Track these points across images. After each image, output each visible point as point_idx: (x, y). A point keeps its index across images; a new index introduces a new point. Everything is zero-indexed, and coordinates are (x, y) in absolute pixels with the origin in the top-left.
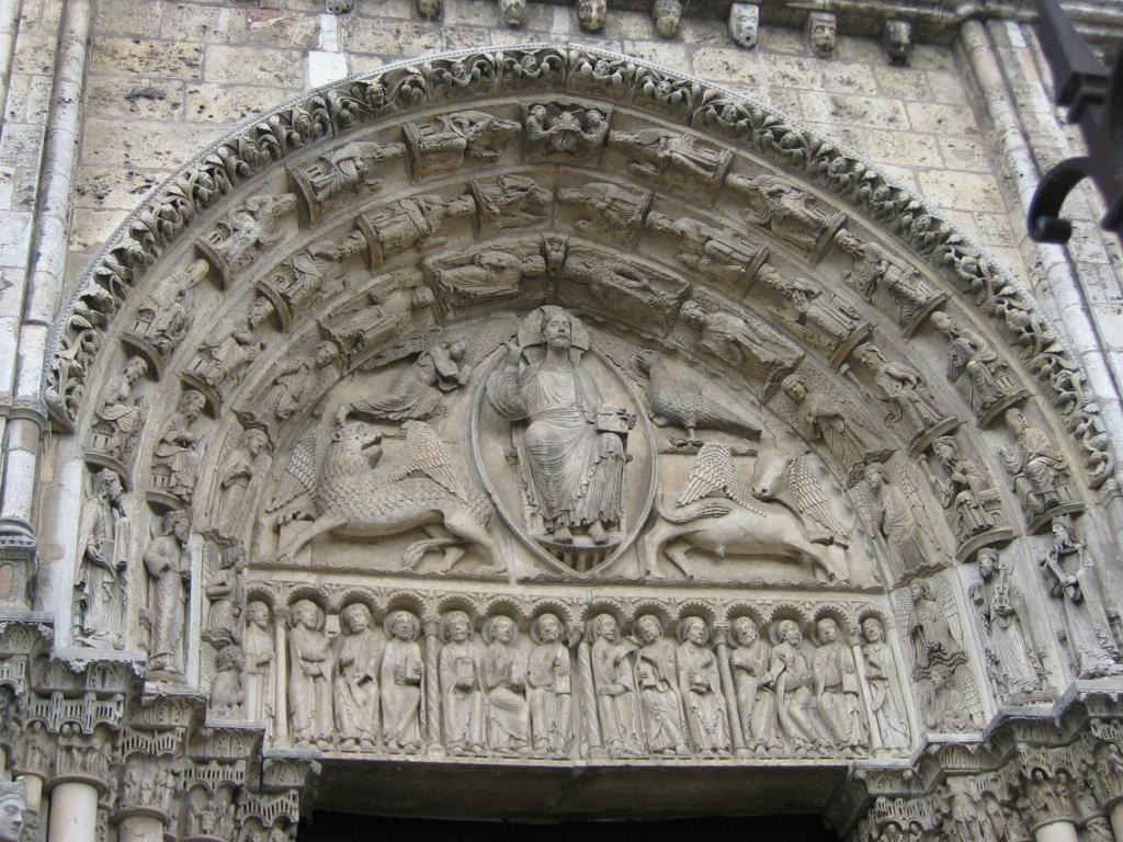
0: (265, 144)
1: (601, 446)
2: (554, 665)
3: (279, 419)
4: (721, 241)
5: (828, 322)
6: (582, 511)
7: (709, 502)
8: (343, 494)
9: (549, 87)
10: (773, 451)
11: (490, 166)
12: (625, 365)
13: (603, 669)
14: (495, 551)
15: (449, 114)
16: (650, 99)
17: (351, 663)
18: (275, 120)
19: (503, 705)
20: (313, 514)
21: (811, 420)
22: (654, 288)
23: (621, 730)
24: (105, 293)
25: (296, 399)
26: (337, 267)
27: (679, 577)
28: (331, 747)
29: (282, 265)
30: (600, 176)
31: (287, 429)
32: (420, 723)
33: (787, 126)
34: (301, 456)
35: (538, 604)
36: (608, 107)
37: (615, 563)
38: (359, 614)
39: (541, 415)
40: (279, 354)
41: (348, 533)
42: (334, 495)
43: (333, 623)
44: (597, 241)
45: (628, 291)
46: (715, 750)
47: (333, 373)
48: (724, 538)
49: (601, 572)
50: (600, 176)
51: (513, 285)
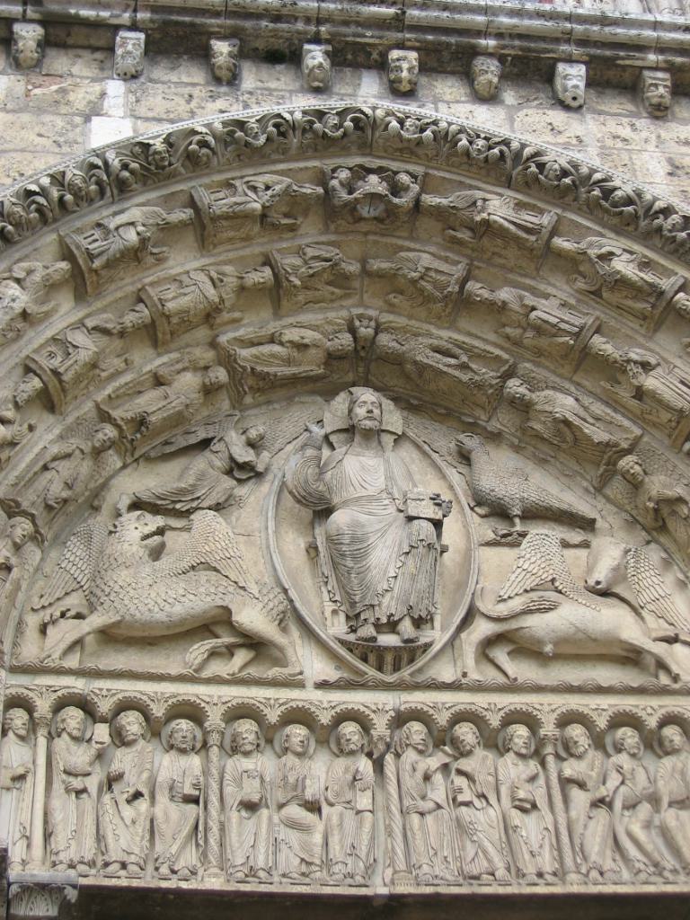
0: (33, 207)
1: (411, 534)
2: (355, 779)
3: (49, 508)
4: (547, 312)
5: (668, 395)
6: (389, 606)
7: (534, 595)
8: (117, 588)
9: (354, 149)
10: (609, 539)
11: (290, 235)
12: (444, 451)
13: (411, 783)
14: (289, 652)
15: (242, 177)
16: (465, 159)
17: (120, 777)
18: (46, 181)
19: (293, 825)
20: (85, 611)
21: (651, 505)
22: (474, 366)
23: (432, 853)
25: (69, 486)
26: (117, 344)
27: (501, 679)
28: (93, 871)
29: (54, 339)
30: (412, 245)
31: (60, 520)
32: (197, 845)
33: (617, 183)
34: (75, 551)
35: (338, 710)
36: (419, 170)
37: (427, 665)
38: (132, 723)
39: (345, 503)
40: (51, 437)
41: (123, 632)
42: (107, 590)
43: (102, 732)
44: (410, 317)
45: (445, 369)
46: (540, 875)
47: (113, 460)
48: (553, 635)
49: (411, 675)
50: (412, 245)
51: (319, 366)
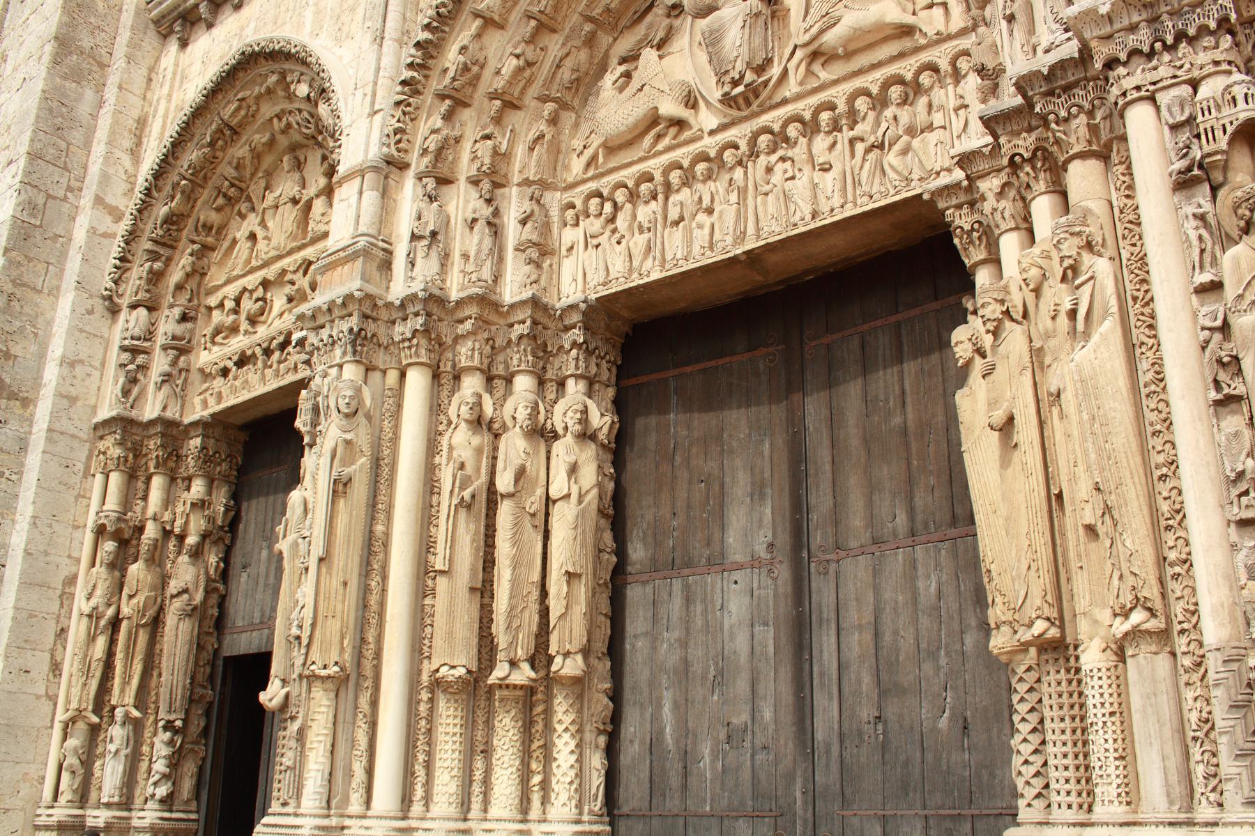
3: (569, 89)
7: (825, 19)
24: (410, 74)
31: (582, 90)
38: (620, 196)
47: (604, 39)
